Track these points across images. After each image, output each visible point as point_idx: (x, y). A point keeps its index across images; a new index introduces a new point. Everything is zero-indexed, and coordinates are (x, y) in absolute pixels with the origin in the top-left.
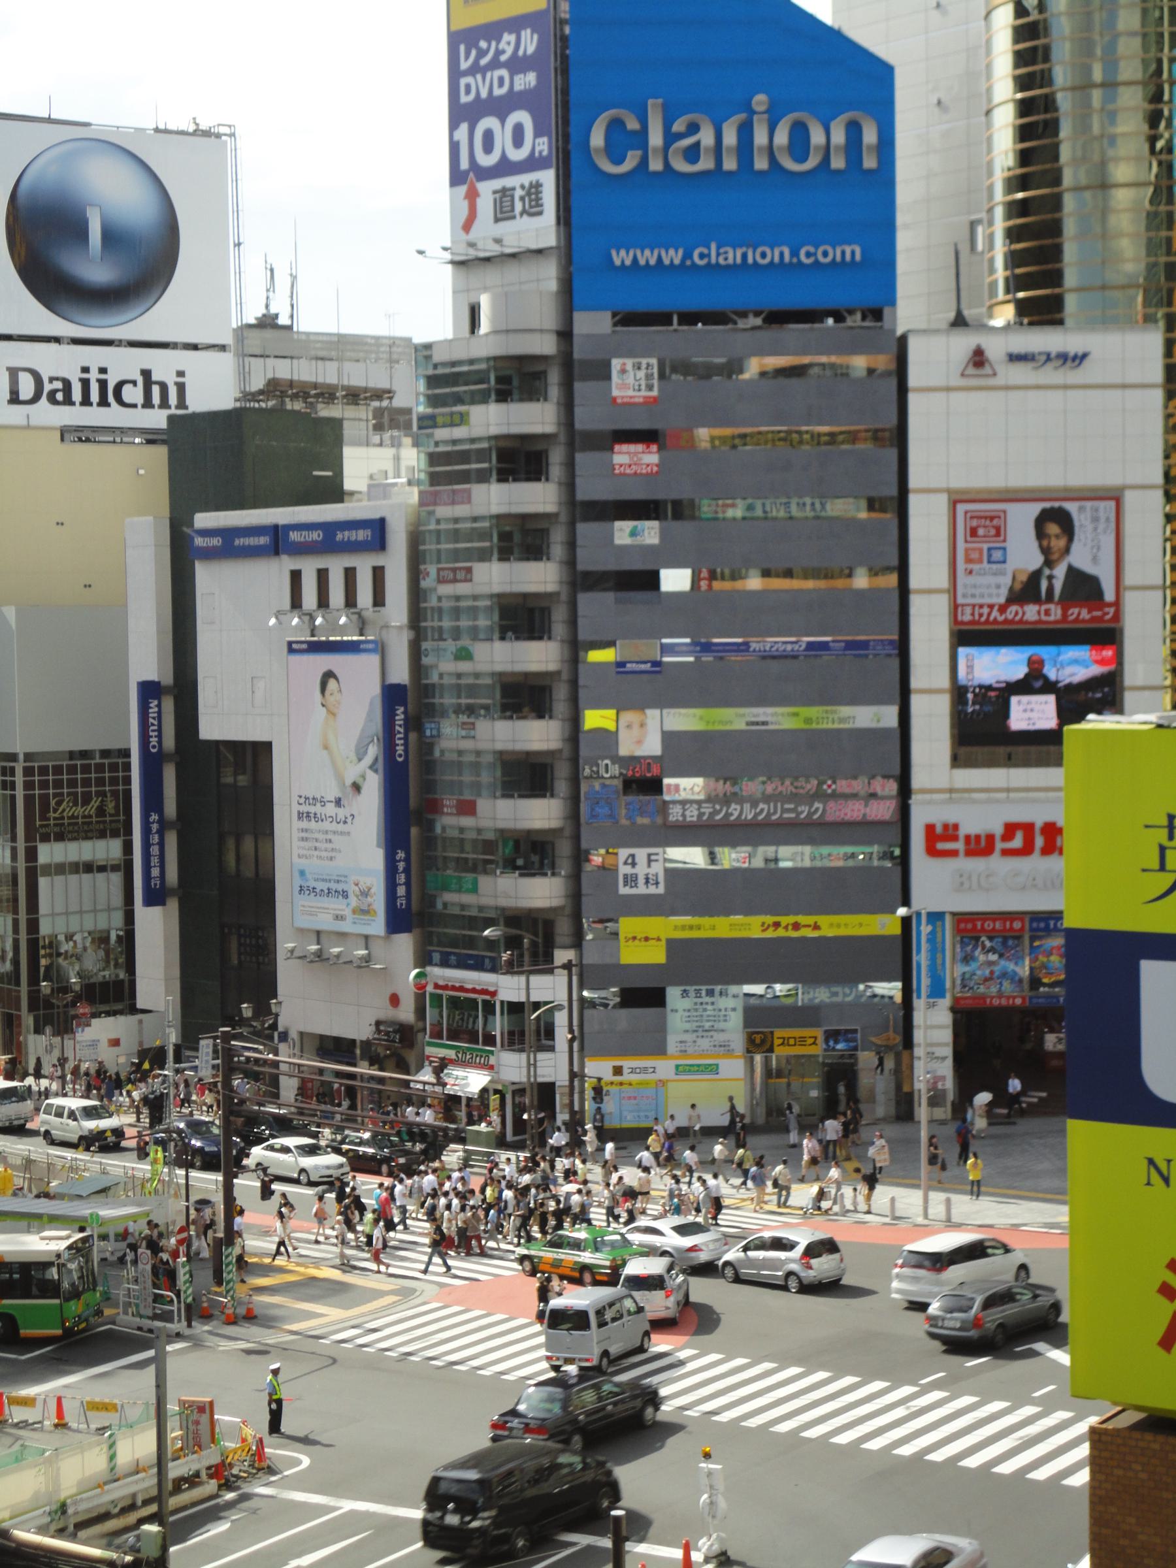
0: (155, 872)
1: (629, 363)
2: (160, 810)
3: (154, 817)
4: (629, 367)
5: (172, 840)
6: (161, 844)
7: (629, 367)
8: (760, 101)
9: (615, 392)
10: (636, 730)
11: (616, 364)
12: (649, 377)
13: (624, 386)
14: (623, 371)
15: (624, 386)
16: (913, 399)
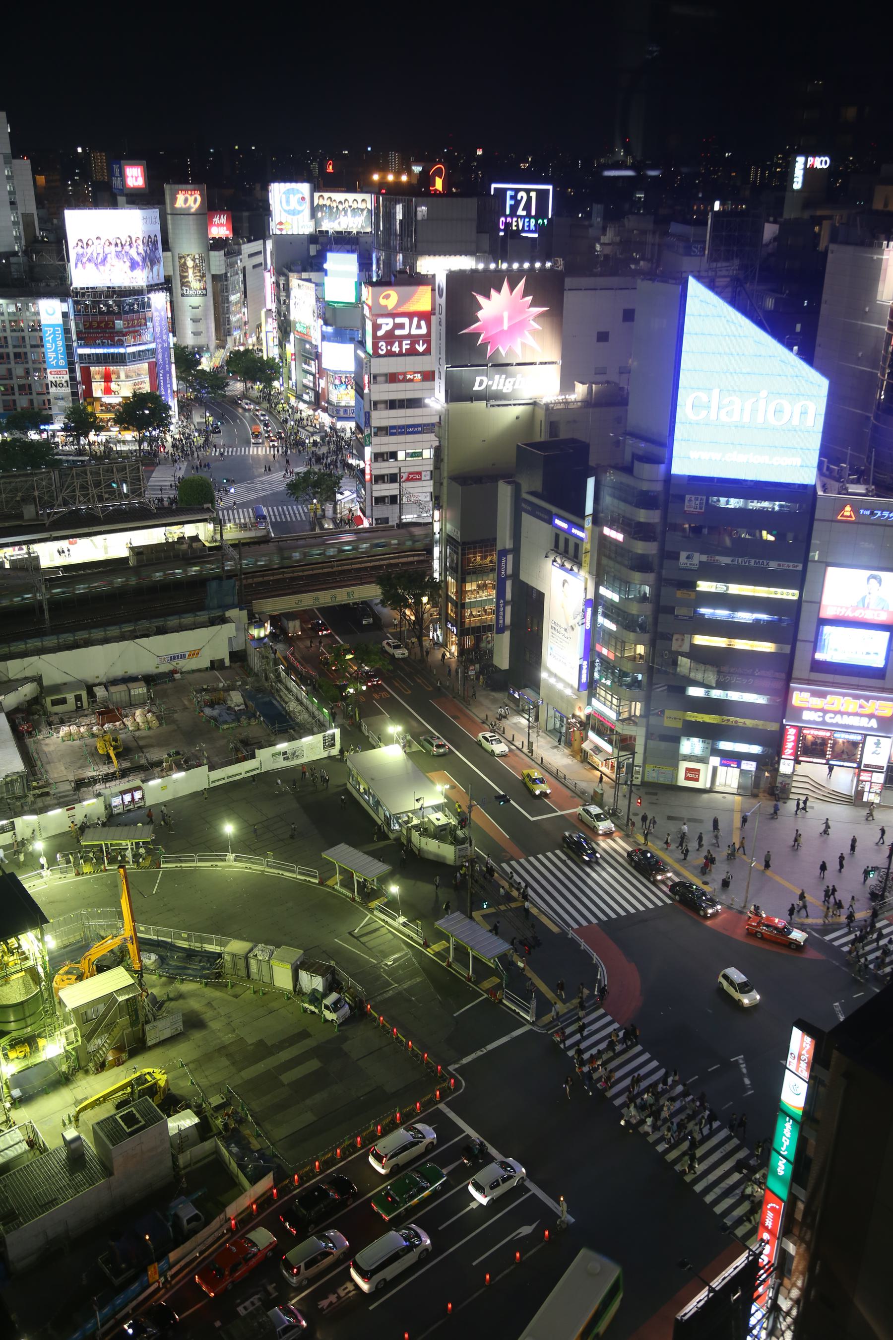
0: (501, 621)
1: (693, 498)
2: (504, 598)
3: (502, 601)
4: (693, 499)
5: (508, 609)
6: (504, 611)
7: (693, 499)
8: (764, 393)
9: (686, 509)
10: (679, 642)
11: (687, 497)
12: (701, 504)
13: (690, 507)
14: (690, 500)
15: (690, 507)
16: (816, 524)
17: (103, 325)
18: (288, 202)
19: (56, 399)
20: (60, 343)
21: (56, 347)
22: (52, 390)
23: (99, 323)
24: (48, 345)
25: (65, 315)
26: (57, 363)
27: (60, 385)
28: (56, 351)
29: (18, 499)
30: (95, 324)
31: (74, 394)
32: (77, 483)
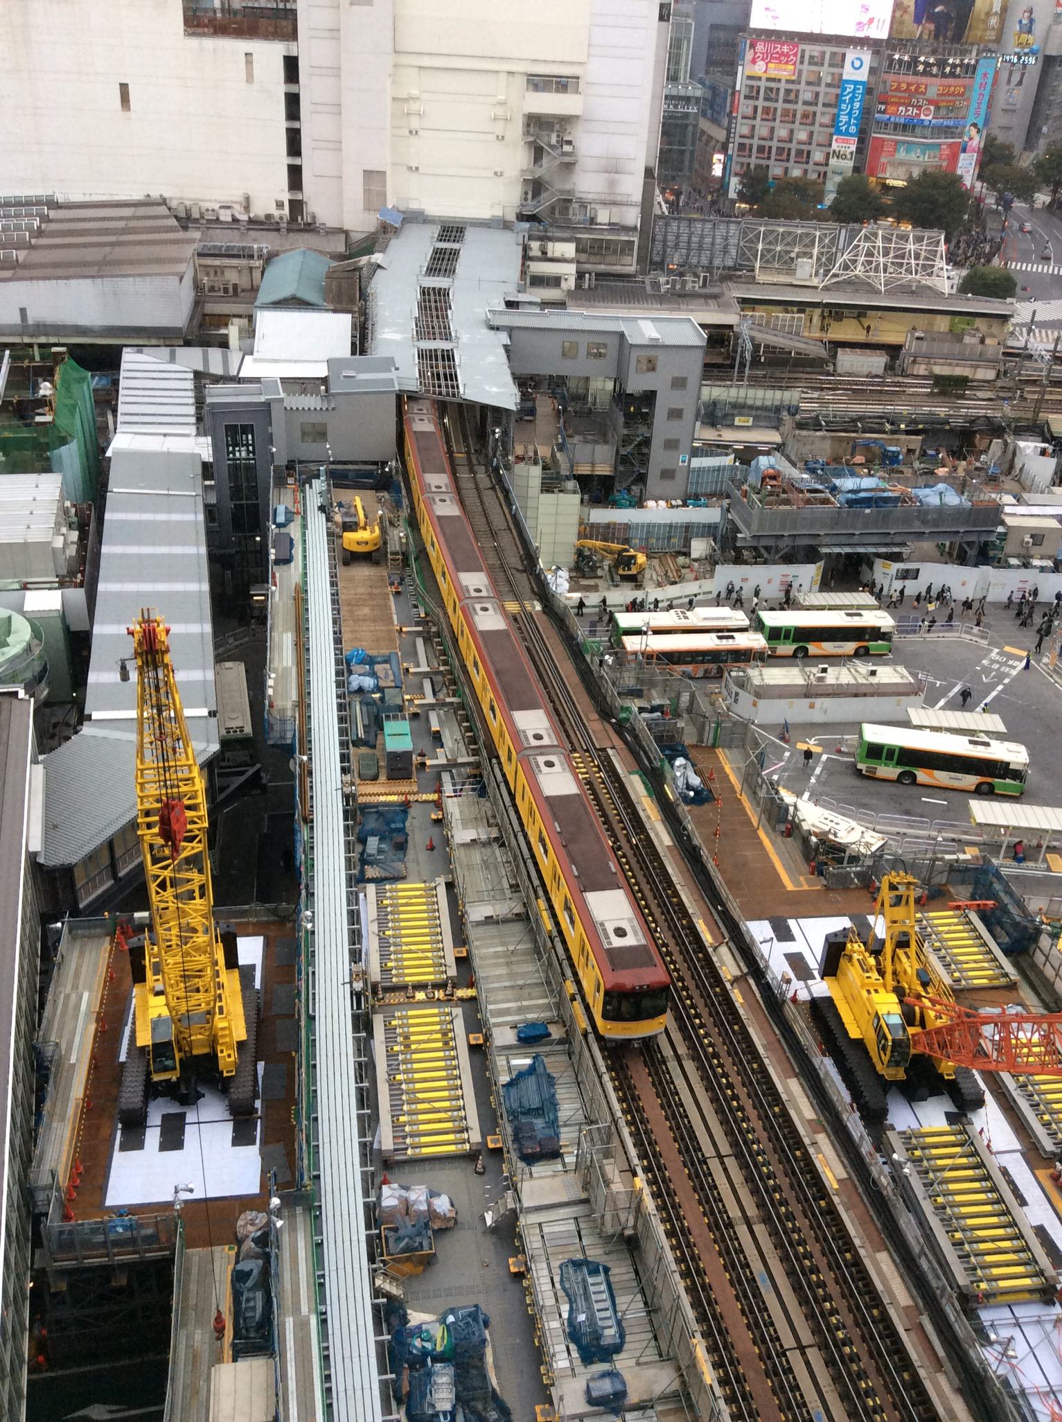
17: (913, 88)
19: (834, 172)
20: (857, 105)
21: (852, 109)
22: (833, 161)
23: (909, 85)
24: (844, 106)
25: (872, 71)
26: (847, 129)
27: (844, 157)
28: (850, 114)
29: (793, 255)
30: (904, 86)
31: (856, 169)
32: (865, 245)
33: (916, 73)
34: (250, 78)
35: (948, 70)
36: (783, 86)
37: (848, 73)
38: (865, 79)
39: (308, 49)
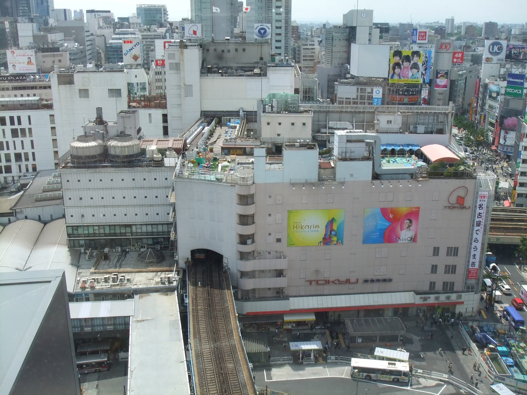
18: (493, 50)
25: (383, 94)
33: (399, 94)
34: (150, 121)
35: (411, 93)
36: (352, 101)
37: (375, 95)
38: (381, 97)
39: (170, 111)
